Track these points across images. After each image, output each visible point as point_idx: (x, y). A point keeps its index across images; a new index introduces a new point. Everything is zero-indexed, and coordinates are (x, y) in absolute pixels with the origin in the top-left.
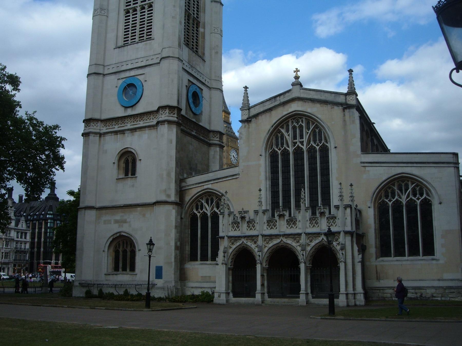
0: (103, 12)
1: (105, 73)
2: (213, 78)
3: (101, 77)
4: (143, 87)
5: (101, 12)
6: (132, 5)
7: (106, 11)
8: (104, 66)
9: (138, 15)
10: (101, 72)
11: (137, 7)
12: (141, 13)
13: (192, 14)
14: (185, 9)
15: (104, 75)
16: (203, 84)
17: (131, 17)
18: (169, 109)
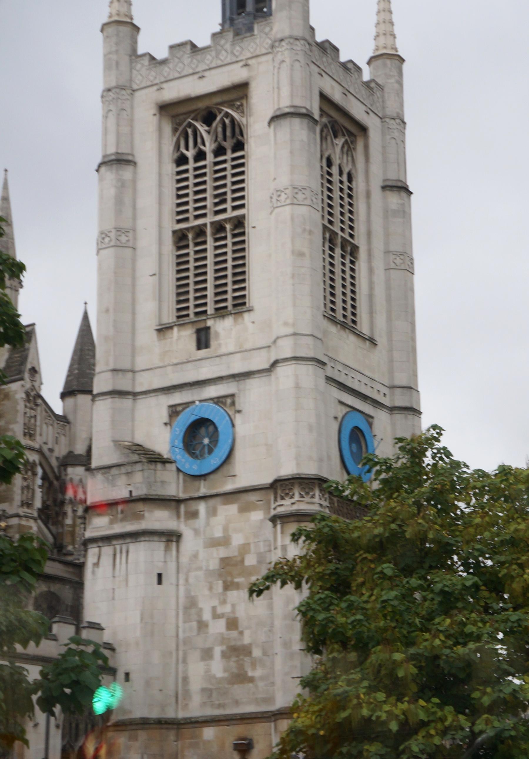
0: (123, 239)
1: (138, 389)
2: (397, 383)
3: (128, 402)
4: (233, 426)
5: (120, 238)
6: (191, 218)
8: (133, 371)
9: (210, 244)
10: (128, 388)
11: (205, 225)
12: (216, 240)
13: (337, 234)
14: (324, 225)
15: (135, 395)
16: (376, 403)
17: (191, 250)
18: (300, 484)
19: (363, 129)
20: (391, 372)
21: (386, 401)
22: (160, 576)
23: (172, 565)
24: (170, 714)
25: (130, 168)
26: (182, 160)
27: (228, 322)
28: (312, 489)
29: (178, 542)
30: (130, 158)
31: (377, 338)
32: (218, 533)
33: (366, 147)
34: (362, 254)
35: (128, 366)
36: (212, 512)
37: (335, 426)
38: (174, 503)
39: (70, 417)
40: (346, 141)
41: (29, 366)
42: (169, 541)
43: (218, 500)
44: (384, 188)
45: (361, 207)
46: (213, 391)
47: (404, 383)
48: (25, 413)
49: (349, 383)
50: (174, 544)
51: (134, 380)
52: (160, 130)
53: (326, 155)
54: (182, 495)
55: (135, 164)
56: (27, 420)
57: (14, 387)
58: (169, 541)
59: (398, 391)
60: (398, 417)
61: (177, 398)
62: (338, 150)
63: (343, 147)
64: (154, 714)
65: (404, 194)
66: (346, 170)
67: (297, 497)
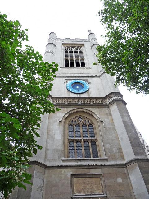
41: (145, 146)
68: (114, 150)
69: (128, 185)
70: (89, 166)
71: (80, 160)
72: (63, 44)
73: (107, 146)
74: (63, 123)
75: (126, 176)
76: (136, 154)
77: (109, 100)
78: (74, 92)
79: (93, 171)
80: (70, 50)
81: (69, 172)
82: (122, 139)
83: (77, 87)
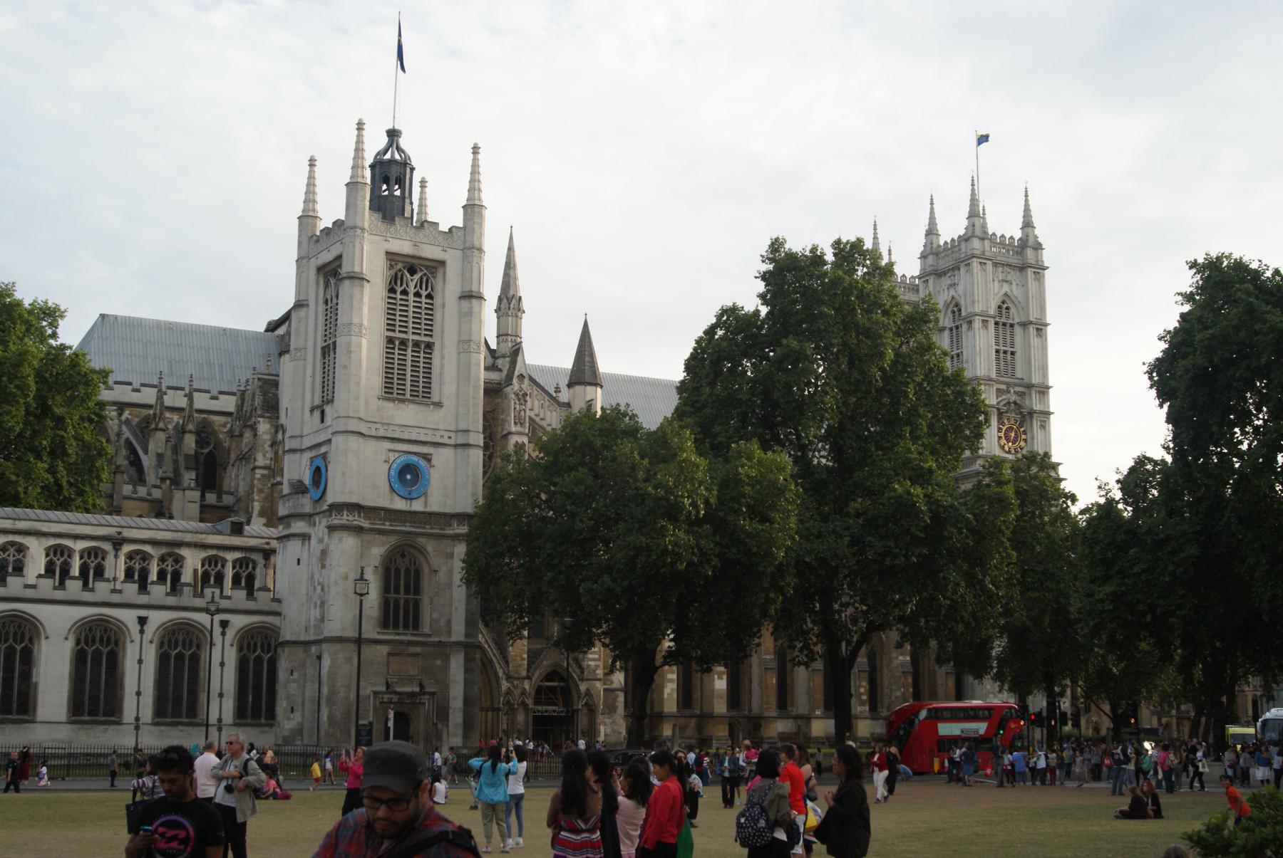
0: (299, 354)
2: (460, 428)
7: (303, 351)
15: (301, 451)
19: (442, 263)
20: (457, 422)
21: (452, 442)
22: (299, 560)
23: (306, 554)
24: (302, 638)
25: (305, 309)
26: (326, 302)
27: (330, 406)
28: (342, 511)
29: (309, 539)
30: (305, 302)
31: (445, 402)
32: (321, 536)
33: (444, 273)
34: (437, 348)
35: (298, 434)
36: (320, 523)
37: (386, 466)
38: (307, 518)
39: (572, 404)
40: (425, 274)
42: (304, 540)
43: (321, 515)
44: (460, 298)
45: (438, 314)
46: (323, 449)
47: (465, 428)
48: (515, 409)
49: (406, 436)
50: (307, 541)
51: (301, 442)
52: (317, 284)
53: (399, 289)
54: (312, 512)
55: (308, 305)
56: (517, 414)
57: (509, 389)
58: (304, 540)
59: (459, 433)
60: (459, 450)
61: (313, 453)
62: (412, 285)
63: (421, 279)
64: (294, 638)
65: (474, 301)
66: (424, 293)
67: (334, 516)
68: (443, 622)
69: (445, 668)
70: (410, 643)
71: (398, 634)
72: (388, 253)
73: (435, 615)
74: (379, 569)
75: (446, 659)
76: (467, 635)
77: (458, 525)
78: (401, 493)
79: (413, 650)
80: (403, 288)
81: (384, 650)
82: (456, 609)
83: (409, 477)
